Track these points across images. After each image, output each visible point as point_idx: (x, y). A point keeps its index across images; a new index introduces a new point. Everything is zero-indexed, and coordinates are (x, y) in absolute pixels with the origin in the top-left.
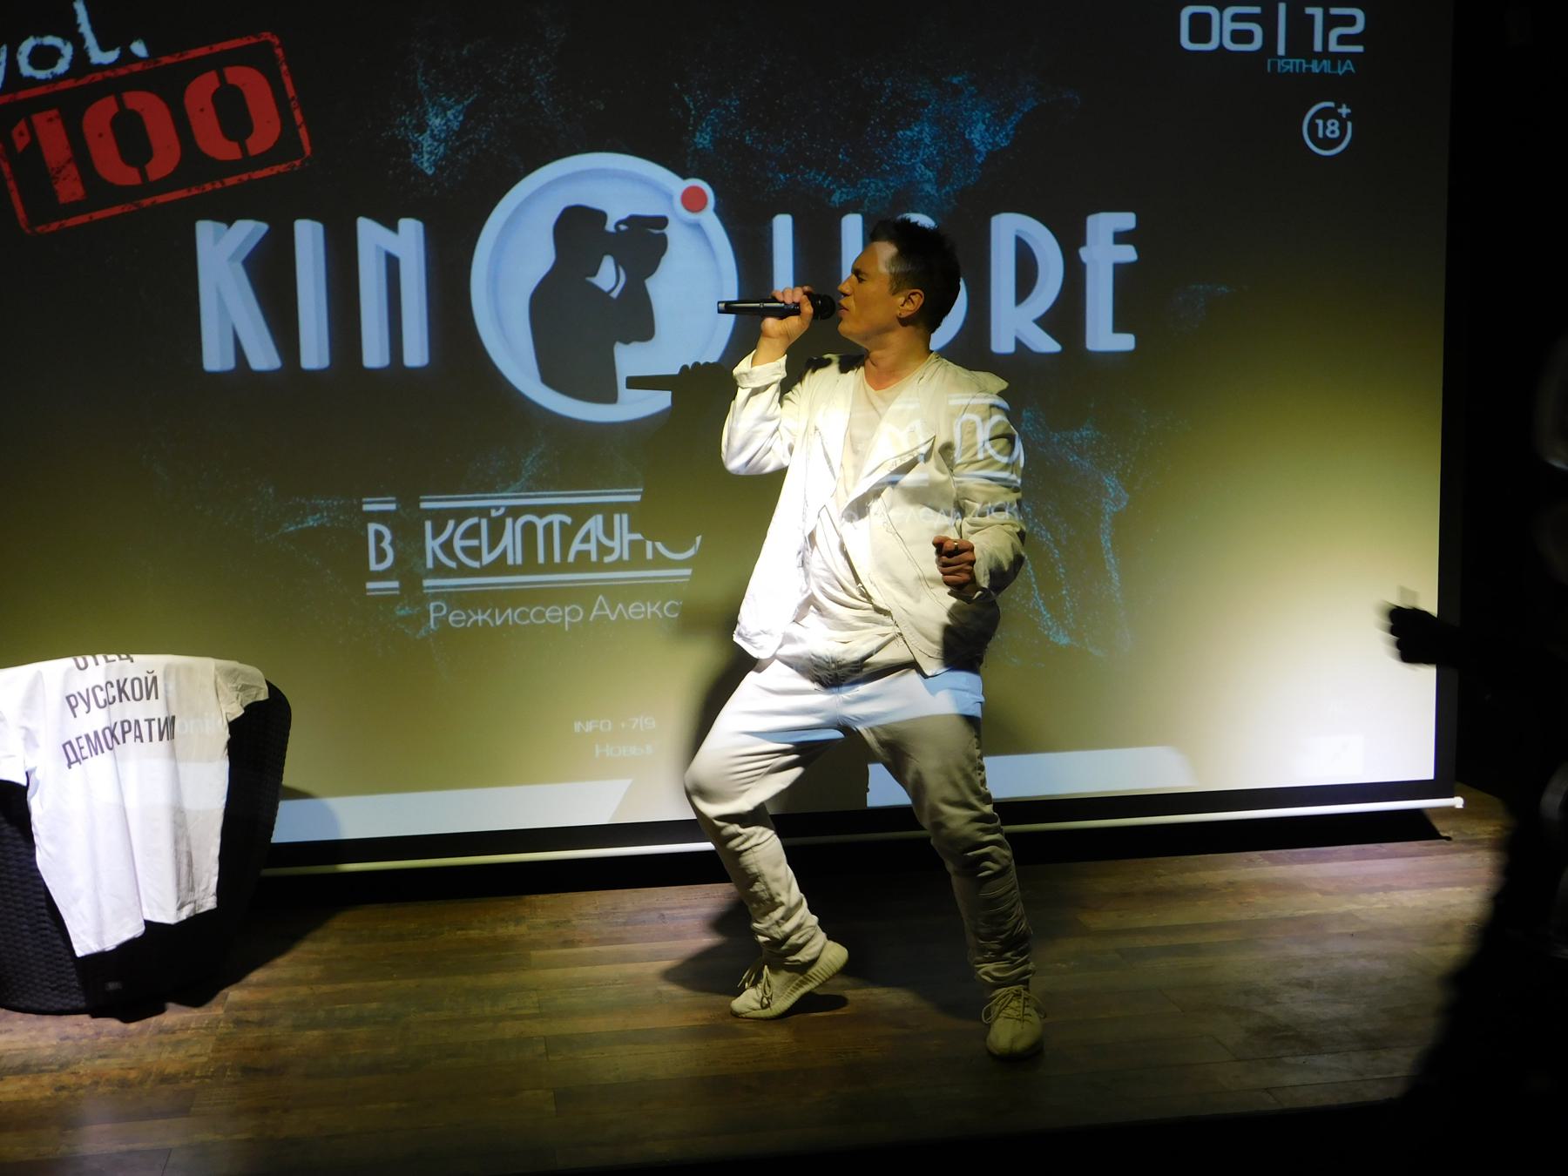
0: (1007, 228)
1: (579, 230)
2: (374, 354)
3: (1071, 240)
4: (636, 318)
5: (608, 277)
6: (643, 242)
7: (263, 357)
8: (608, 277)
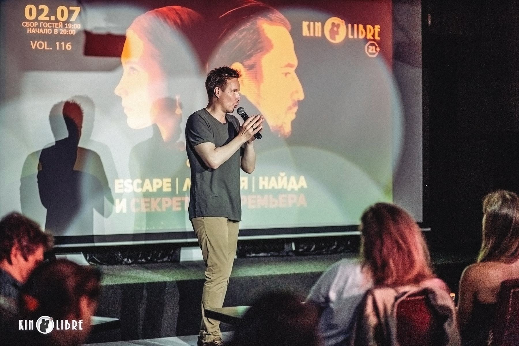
4: (337, 33)
7: (308, 35)
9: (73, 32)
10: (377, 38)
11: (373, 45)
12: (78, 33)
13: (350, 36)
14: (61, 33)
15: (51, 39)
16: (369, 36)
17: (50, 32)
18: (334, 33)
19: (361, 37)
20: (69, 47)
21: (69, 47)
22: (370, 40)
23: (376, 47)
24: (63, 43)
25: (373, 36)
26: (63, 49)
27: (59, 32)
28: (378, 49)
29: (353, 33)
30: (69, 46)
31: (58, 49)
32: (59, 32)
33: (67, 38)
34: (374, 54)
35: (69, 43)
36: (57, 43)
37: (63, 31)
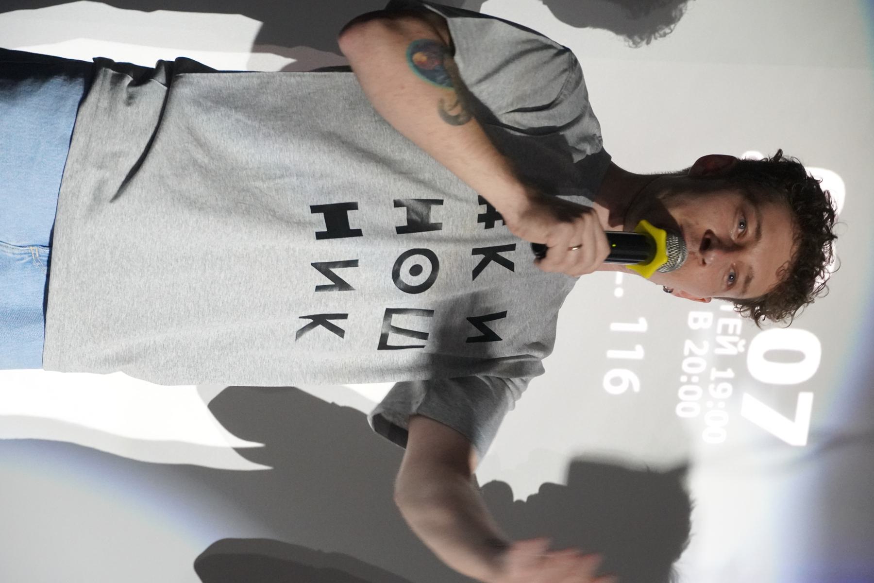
9: (689, 406)
14: (689, 345)
20: (616, 381)
21: (616, 381)
24: (638, 353)
26: (612, 354)
30: (622, 381)
31: (615, 327)
35: (637, 388)
36: (642, 326)
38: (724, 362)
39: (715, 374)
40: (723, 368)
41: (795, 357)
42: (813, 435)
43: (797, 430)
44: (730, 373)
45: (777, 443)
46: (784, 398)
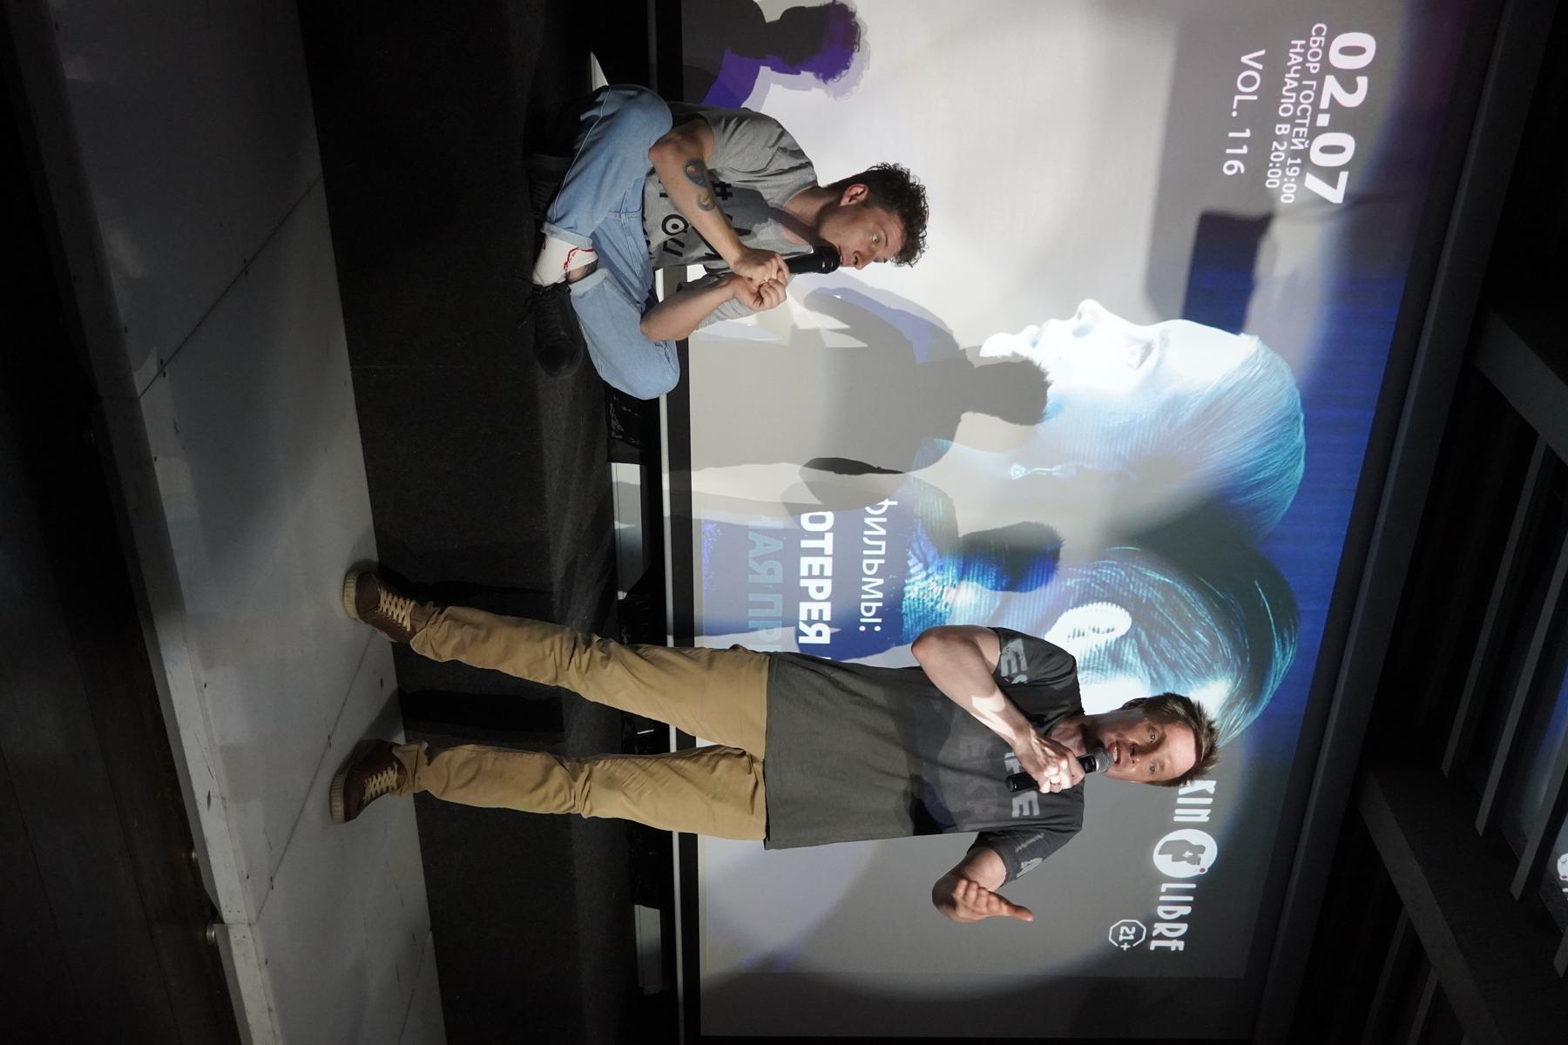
0: (1184, 927)
1: (1202, 849)
2: (1178, 811)
3: (1179, 938)
5: (1188, 854)
6: (1195, 860)
8: (1188, 854)
9: (1273, 180)
10: (1154, 945)
11: (1138, 935)
12: (1271, 196)
13: (1164, 887)
14: (1275, 144)
15: (1263, 116)
16: (1160, 928)
17: (1286, 110)
18: (1177, 851)
19: (1160, 911)
20: (1231, 168)
21: (1231, 168)
22: (1151, 929)
23: (1130, 942)
24: (1245, 150)
25: (1161, 937)
26: (1229, 151)
27: (1280, 139)
28: (1125, 947)
29: (1170, 892)
30: (1234, 167)
31: (1231, 135)
32: (1280, 139)
33: (1259, 162)
34: (1116, 937)
36: (1247, 134)
37: (1279, 152)
38: (1295, 154)
39: (1290, 161)
40: (1294, 158)
41: (1338, 150)
42: (1346, 196)
43: (1336, 195)
44: (1299, 161)
45: (1324, 202)
46: (1330, 175)
